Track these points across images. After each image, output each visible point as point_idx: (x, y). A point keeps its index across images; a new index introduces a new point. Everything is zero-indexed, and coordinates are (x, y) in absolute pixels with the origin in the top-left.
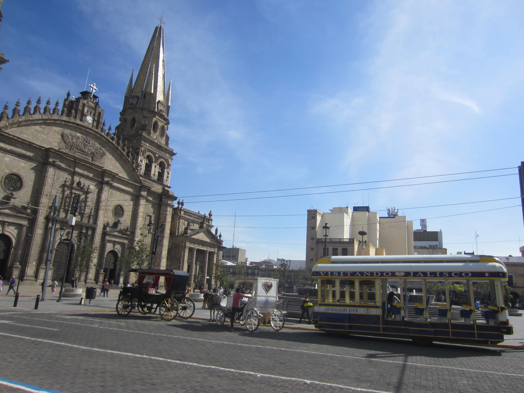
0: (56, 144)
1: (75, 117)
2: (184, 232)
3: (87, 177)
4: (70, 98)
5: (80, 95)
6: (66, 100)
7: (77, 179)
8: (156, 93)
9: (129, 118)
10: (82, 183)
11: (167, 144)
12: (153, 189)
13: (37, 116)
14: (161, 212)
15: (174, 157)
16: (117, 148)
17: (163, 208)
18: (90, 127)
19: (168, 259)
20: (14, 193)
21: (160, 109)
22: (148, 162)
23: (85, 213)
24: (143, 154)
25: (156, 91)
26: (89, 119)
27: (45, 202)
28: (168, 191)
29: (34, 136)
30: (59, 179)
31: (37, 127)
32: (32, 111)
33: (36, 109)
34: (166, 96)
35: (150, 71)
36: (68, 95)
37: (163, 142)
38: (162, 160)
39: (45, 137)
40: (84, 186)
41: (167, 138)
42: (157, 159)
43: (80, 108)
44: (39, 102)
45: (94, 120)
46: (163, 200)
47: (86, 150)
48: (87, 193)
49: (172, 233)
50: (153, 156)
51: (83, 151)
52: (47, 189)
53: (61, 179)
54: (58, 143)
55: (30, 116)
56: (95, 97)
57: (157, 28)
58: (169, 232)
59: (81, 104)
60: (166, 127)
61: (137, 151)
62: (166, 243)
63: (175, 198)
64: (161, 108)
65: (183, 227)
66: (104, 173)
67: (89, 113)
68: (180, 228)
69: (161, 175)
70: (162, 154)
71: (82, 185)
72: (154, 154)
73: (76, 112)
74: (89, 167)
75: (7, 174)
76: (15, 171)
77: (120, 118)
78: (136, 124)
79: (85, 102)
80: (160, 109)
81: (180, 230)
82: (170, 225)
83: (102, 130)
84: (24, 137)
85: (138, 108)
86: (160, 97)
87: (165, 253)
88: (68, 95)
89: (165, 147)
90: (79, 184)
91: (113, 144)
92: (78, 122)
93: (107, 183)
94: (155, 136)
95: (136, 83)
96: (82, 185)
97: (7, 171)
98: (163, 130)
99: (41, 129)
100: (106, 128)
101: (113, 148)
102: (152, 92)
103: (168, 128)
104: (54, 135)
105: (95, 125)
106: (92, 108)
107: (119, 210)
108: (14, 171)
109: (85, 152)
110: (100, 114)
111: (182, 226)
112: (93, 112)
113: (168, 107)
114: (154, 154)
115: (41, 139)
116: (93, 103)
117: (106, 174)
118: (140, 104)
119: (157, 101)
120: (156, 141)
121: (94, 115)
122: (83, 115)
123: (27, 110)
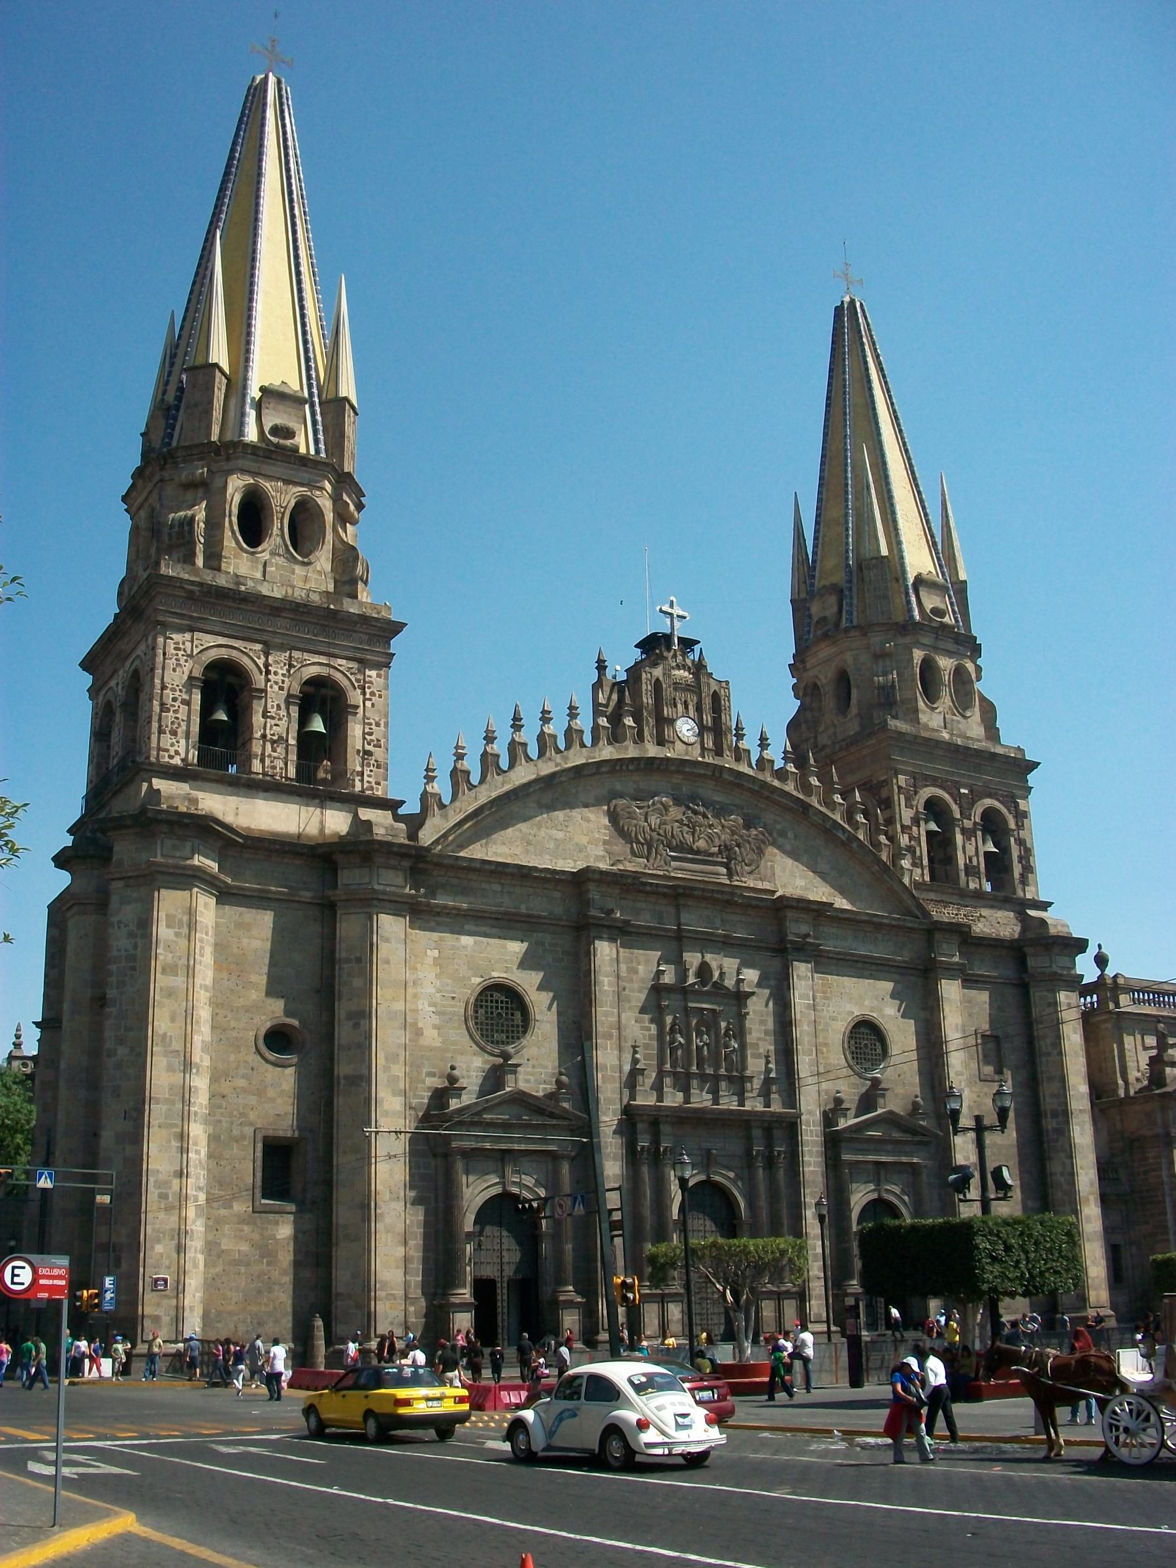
1: (640, 738)
2: (1150, 1079)
3: (726, 945)
4: (609, 674)
5: (637, 654)
6: (597, 686)
7: (693, 959)
8: (901, 551)
9: (825, 676)
10: (714, 965)
11: (992, 733)
12: (980, 928)
13: (523, 774)
14: (1035, 1012)
15: (1032, 778)
16: (806, 807)
17: (1036, 994)
18: (695, 754)
19: (1105, 1201)
20: (510, 1049)
21: (928, 605)
22: (933, 826)
23: (748, 1073)
24: (908, 800)
25: (899, 543)
26: (686, 728)
27: (608, 1061)
28: (1043, 922)
29: (529, 843)
30: (636, 972)
32: (504, 763)
33: (516, 749)
34: (944, 553)
35: (855, 476)
36: (601, 666)
37: (973, 729)
38: (988, 802)
40: (722, 974)
41: (989, 712)
42: (966, 806)
43: (648, 699)
44: (517, 724)
45: (702, 729)
46: (1031, 962)
47: (701, 844)
48: (740, 997)
49: (1099, 1091)
50: (947, 797)
51: (691, 850)
52: (606, 1014)
54: (605, 842)
55: (500, 778)
56: (688, 644)
57: (839, 311)
58: (1084, 1089)
59: (646, 687)
60: (970, 666)
61: (884, 793)
62: (1083, 1135)
63: (1080, 945)
64: (931, 601)
65: (1144, 1058)
66: (781, 908)
67: (680, 707)
68: (1131, 1064)
69: (997, 866)
71: (716, 974)
72: (952, 788)
73: (638, 719)
74: (727, 900)
75: (479, 989)
76: (497, 975)
77: (794, 687)
78: (854, 693)
79: (658, 672)
80: (928, 605)
81: (1133, 1074)
82: (1082, 1060)
83: (740, 754)
85: (847, 630)
86: (918, 560)
87: (1087, 1178)
88: (601, 666)
89: (984, 745)
90: (704, 971)
91: (787, 794)
92: (652, 750)
94: (935, 719)
95: (816, 538)
96: (716, 974)
98: (963, 681)
100: (750, 743)
101: (790, 810)
102: (884, 551)
103: (979, 669)
104: (588, 821)
105: (709, 743)
106: (687, 688)
108: (495, 974)
109: (698, 852)
110: (716, 697)
111: (1137, 1054)
112: (692, 700)
113: (961, 589)
115: (552, 845)
116: (684, 667)
117: (790, 914)
118: (850, 613)
119: (911, 580)
120: (945, 735)
121: (699, 709)
122: (664, 723)
123: (488, 761)
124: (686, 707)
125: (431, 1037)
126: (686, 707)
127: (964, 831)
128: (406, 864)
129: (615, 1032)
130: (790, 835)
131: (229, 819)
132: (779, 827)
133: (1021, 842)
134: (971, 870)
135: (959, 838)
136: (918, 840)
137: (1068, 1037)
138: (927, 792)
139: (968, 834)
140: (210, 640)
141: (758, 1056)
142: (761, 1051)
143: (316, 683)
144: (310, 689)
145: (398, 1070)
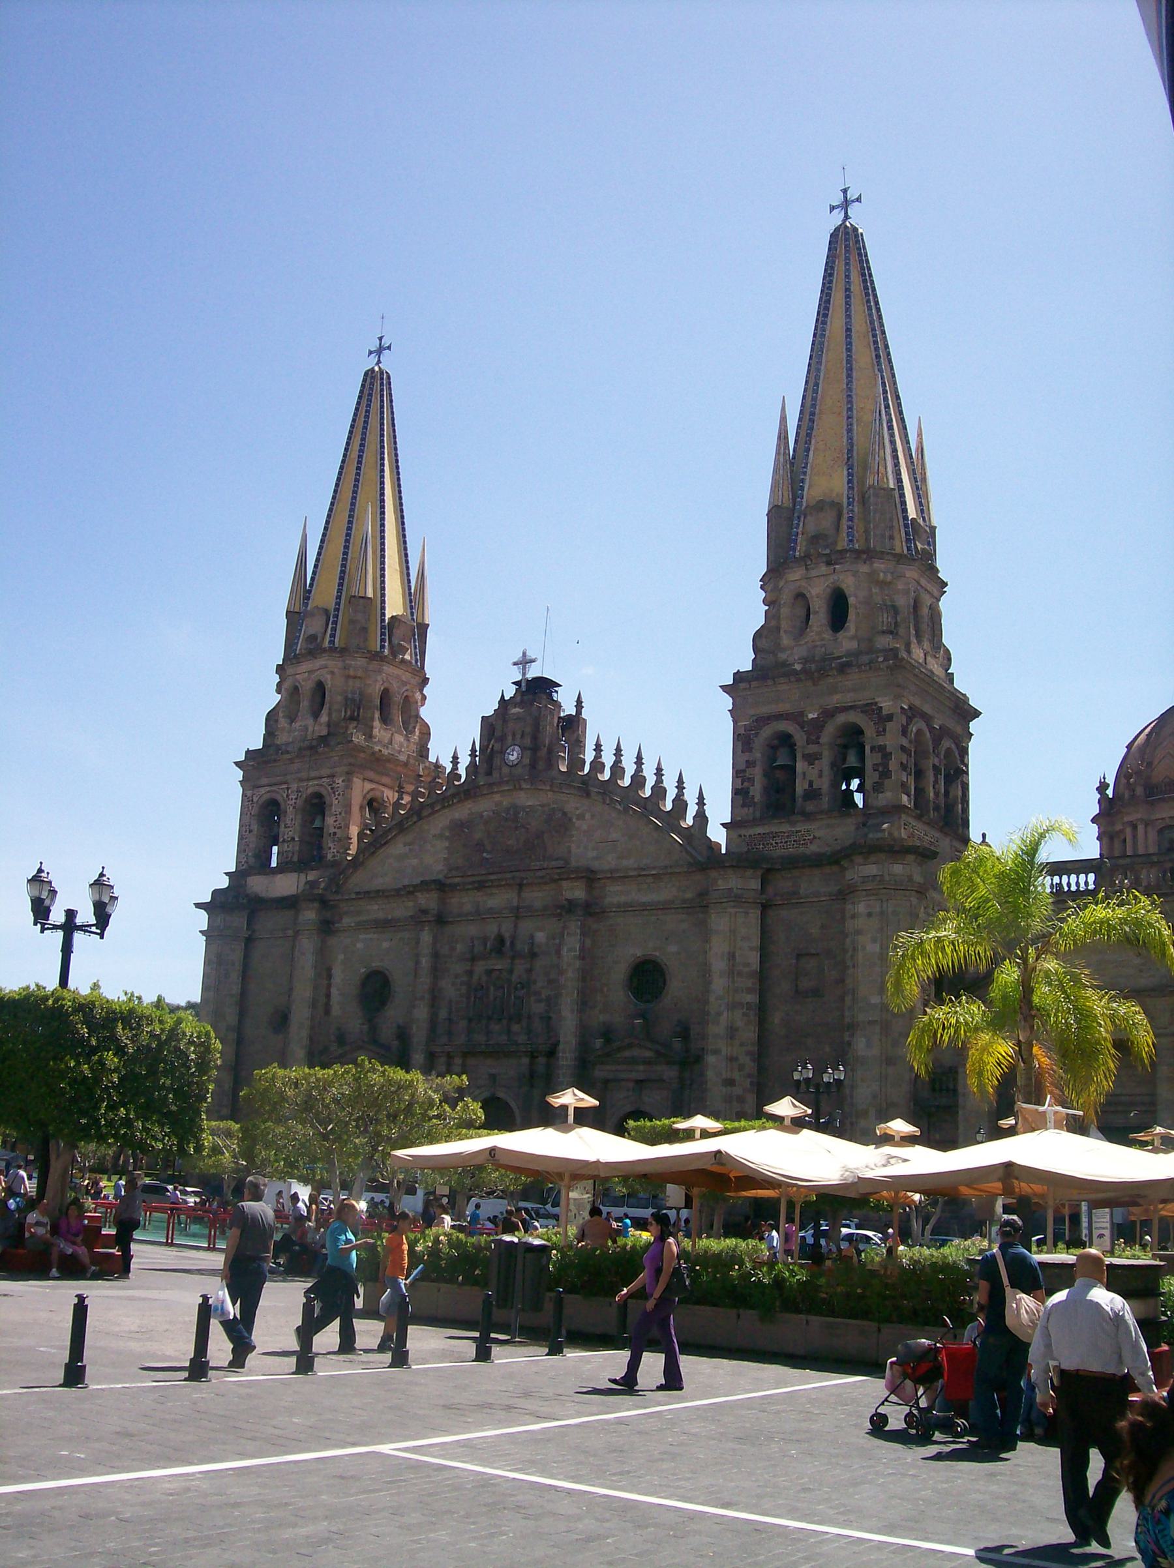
0: (440, 867)
10: (507, 935)
31: (398, 848)
38: (841, 719)
39: (415, 862)
40: (512, 943)
45: (523, 749)
53: (459, 947)
70: (845, 692)
71: (508, 943)
76: (376, 964)
84: (379, 883)
90: (501, 940)
93: (570, 907)
96: (508, 943)
97: (363, 970)
99: (407, 848)
105: (527, 761)
106: (518, 718)
107: (647, 978)
114: (797, 717)
117: (565, 884)
120: (798, 667)
121: (522, 736)
124: (514, 735)
125: (336, 1010)
126: (514, 735)
127: (806, 757)
128: (316, 905)
129: (427, 996)
130: (588, 816)
131: (263, 895)
132: (578, 812)
133: (882, 749)
134: (812, 794)
135: (800, 766)
136: (751, 780)
137: (864, 948)
138: (767, 732)
139: (811, 759)
140: (263, 790)
141: (540, 1001)
142: (543, 996)
143: (319, 796)
144: (315, 801)
145: (304, 1033)
